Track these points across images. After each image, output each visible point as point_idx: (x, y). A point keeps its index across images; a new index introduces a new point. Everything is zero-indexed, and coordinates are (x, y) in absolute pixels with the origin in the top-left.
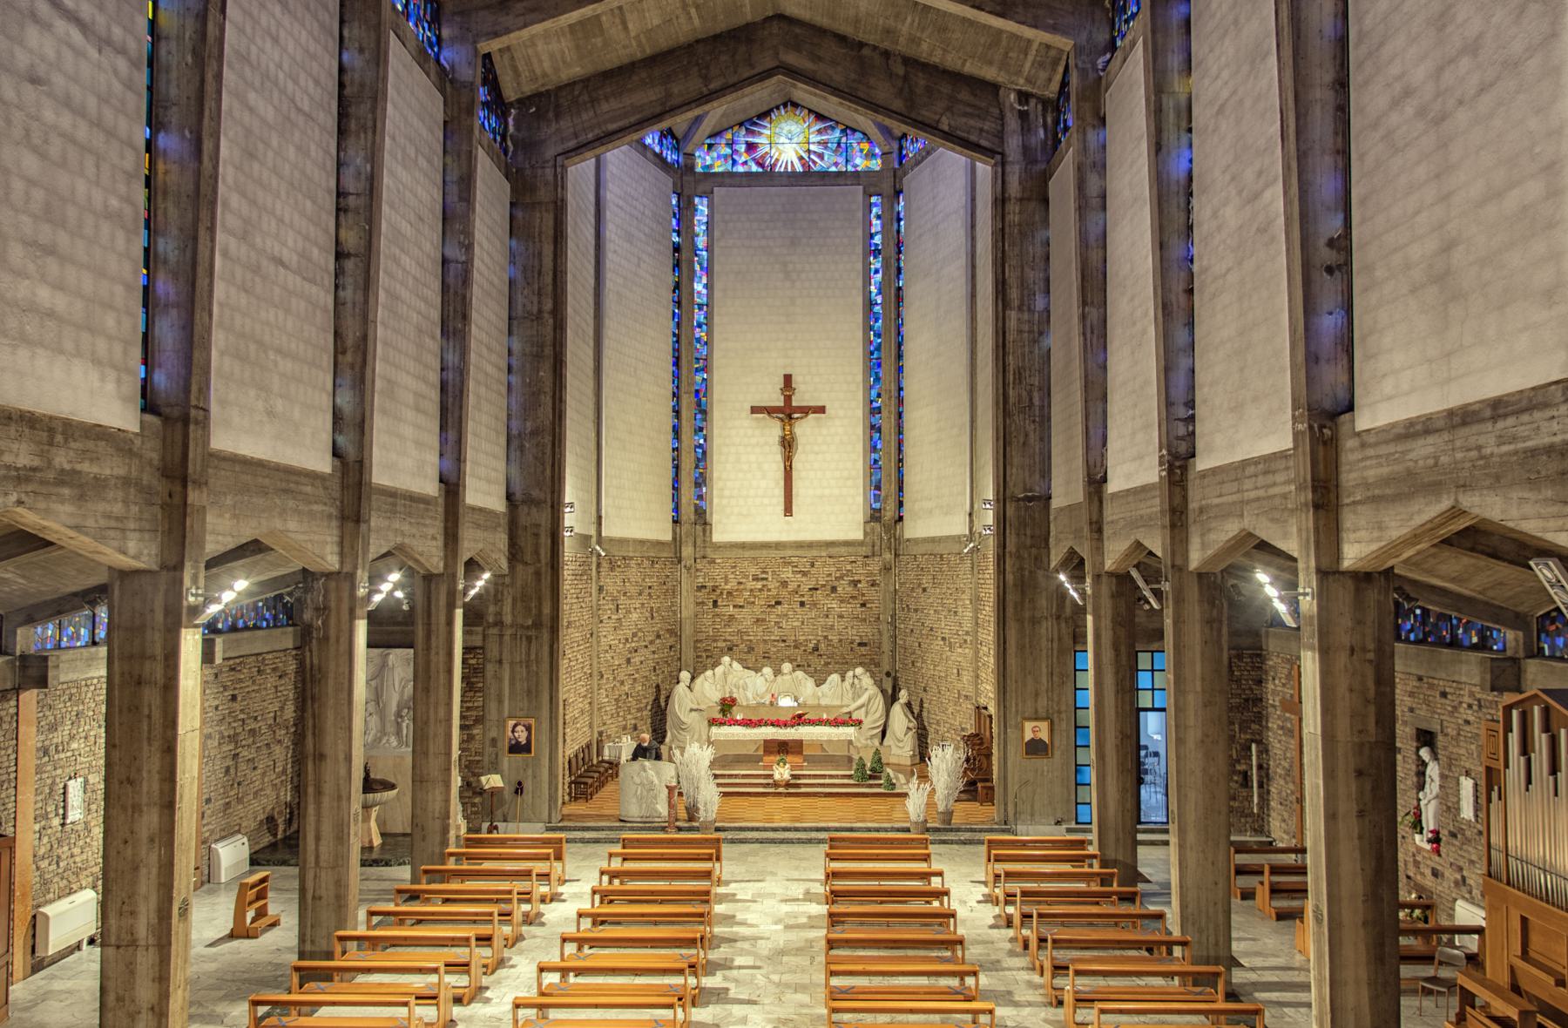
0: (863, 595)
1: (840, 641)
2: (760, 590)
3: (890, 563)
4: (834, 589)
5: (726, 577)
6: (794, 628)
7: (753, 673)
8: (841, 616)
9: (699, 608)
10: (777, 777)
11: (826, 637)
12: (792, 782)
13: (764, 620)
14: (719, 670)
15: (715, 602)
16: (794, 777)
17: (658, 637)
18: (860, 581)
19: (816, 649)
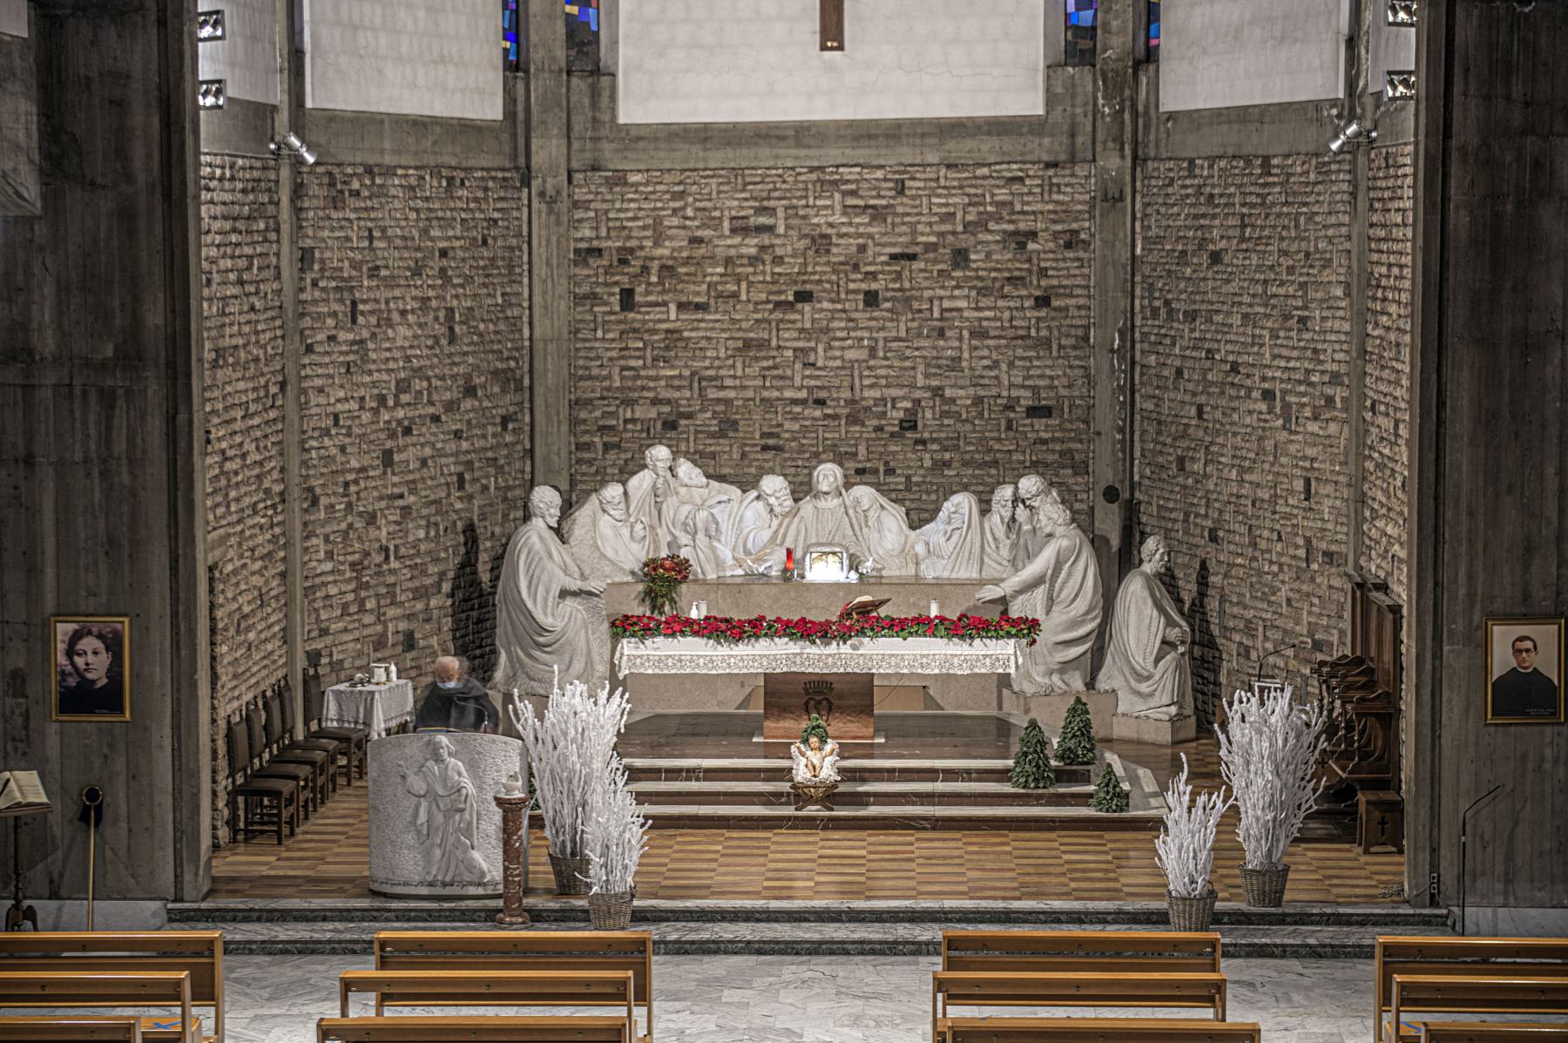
0: (1043, 273)
1: (978, 401)
2: (753, 260)
3: (1118, 181)
4: (960, 257)
5: (658, 221)
6: (849, 366)
7: (735, 492)
8: (980, 333)
9: (581, 312)
10: (802, 774)
11: (937, 392)
12: (842, 788)
13: (764, 344)
14: (641, 482)
16: (849, 774)
17: (470, 391)
18: (1033, 235)
19: (909, 424)
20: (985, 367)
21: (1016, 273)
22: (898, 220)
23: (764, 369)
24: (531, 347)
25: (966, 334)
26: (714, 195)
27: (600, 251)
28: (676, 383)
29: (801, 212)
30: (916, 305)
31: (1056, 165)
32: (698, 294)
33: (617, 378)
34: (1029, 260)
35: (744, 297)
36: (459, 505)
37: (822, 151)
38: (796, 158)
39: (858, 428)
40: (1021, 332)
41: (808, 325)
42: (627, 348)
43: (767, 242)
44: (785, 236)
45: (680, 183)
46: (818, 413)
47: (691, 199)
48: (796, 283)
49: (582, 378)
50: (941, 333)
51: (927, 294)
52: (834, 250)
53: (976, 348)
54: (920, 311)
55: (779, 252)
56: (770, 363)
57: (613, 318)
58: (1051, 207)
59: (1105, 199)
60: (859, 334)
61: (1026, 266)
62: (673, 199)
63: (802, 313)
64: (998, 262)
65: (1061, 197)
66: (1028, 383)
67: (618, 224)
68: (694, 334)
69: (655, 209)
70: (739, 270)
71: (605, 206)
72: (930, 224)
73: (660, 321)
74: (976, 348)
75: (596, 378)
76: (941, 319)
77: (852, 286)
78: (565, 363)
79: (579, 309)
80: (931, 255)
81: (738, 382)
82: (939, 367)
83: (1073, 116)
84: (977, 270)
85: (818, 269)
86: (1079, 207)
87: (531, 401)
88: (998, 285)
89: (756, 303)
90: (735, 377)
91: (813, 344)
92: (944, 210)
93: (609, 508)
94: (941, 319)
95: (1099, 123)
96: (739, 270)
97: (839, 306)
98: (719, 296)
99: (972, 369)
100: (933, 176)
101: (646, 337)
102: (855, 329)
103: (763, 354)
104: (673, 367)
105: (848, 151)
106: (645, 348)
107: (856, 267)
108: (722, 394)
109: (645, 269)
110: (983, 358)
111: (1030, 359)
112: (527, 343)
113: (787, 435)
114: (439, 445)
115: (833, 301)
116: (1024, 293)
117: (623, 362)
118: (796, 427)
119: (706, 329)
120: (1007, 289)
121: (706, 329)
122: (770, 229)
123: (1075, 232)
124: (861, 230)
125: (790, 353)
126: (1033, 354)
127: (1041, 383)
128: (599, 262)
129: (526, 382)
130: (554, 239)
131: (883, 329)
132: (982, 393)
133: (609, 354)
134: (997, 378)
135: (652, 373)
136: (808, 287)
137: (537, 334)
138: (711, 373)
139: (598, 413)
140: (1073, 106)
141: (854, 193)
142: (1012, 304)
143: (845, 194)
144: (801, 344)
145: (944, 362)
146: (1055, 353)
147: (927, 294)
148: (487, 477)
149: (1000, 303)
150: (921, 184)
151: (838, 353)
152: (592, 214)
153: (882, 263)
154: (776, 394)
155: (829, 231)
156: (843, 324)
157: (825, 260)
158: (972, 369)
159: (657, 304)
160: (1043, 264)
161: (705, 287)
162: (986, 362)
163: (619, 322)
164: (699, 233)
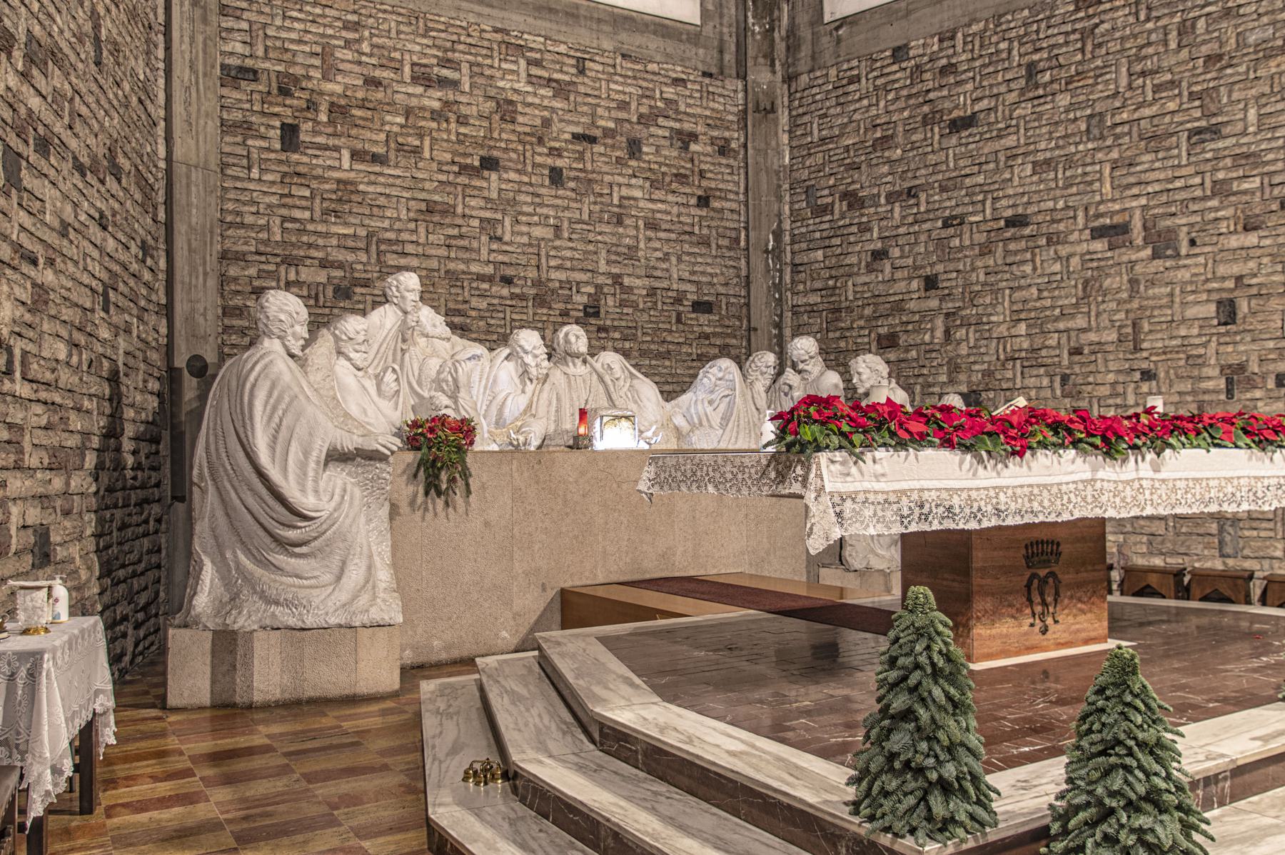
0: (702, 174)
1: (652, 292)
2: (436, 115)
4: (634, 147)
6: (536, 243)
8: (652, 225)
11: (617, 279)
13: (448, 211)
15: (290, 134)
18: (693, 137)
21: (682, 171)
22: (579, 99)
23: (450, 237)
24: (169, 172)
25: (641, 223)
26: (393, 34)
27: (255, 72)
28: (350, 243)
29: (488, 72)
30: (597, 189)
31: (711, 75)
32: (376, 142)
34: (692, 160)
35: (427, 154)
37: (506, 14)
38: (479, 15)
39: (545, 311)
40: (687, 228)
41: (494, 195)
42: (290, 195)
43: (451, 97)
44: (471, 94)
45: (355, 12)
46: (505, 292)
47: (366, 33)
48: (482, 146)
49: (231, 225)
50: (620, 223)
51: (607, 178)
52: (520, 119)
53: (650, 239)
54: (601, 195)
55: (464, 110)
56: (455, 232)
57: (273, 156)
58: (708, 113)
59: (757, 110)
60: (545, 211)
61: (689, 165)
62: (345, 28)
63: (487, 180)
64: (666, 158)
65: (716, 106)
66: (693, 278)
67: (278, 44)
68: (371, 189)
69: (323, 35)
70: (423, 123)
71: (262, 19)
72: (609, 109)
73: (330, 168)
74: (650, 239)
75: (251, 226)
76: (620, 206)
77: (538, 159)
78: (213, 200)
79: (228, 139)
80: (609, 141)
82: (618, 254)
83: (721, 33)
84: (649, 162)
85: (504, 136)
86: (730, 118)
88: (667, 179)
89: (440, 163)
90: (416, 243)
91: (499, 216)
92: (622, 97)
93: (348, 349)
94: (620, 206)
95: (749, 40)
96: (423, 123)
97: (526, 179)
98: (400, 147)
100: (610, 61)
101: (314, 184)
102: (541, 205)
104: (346, 224)
105: (530, 20)
106: (312, 197)
107: (540, 141)
109: (311, 106)
110: (656, 250)
112: (162, 165)
113: (473, 313)
114: (83, 217)
115: (518, 171)
116: (688, 190)
117: (284, 212)
118: (483, 304)
119: (385, 185)
120: (674, 186)
121: (385, 185)
122: (455, 84)
123: (727, 140)
124: (546, 103)
125: (476, 223)
126: (696, 250)
127: (704, 279)
128: (253, 86)
130: (200, 38)
131: (568, 208)
132: (657, 284)
133: (267, 199)
134: (667, 270)
135: (321, 228)
136: (495, 153)
137: (178, 153)
139: (252, 271)
140: (721, 24)
141: (537, 63)
142: (679, 199)
143: (530, 62)
144: (488, 214)
146: (714, 252)
147: (607, 178)
149: (670, 198)
150: (600, 68)
151: (525, 229)
152: (245, 26)
153: (566, 141)
154: (462, 267)
155: (515, 98)
156: (529, 199)
157: (510, 127)
159: (326, 148)
160: (703, 167)
161: (382, 137)
162: (658, 254)
163: (280, 162)
164: (378, 73)
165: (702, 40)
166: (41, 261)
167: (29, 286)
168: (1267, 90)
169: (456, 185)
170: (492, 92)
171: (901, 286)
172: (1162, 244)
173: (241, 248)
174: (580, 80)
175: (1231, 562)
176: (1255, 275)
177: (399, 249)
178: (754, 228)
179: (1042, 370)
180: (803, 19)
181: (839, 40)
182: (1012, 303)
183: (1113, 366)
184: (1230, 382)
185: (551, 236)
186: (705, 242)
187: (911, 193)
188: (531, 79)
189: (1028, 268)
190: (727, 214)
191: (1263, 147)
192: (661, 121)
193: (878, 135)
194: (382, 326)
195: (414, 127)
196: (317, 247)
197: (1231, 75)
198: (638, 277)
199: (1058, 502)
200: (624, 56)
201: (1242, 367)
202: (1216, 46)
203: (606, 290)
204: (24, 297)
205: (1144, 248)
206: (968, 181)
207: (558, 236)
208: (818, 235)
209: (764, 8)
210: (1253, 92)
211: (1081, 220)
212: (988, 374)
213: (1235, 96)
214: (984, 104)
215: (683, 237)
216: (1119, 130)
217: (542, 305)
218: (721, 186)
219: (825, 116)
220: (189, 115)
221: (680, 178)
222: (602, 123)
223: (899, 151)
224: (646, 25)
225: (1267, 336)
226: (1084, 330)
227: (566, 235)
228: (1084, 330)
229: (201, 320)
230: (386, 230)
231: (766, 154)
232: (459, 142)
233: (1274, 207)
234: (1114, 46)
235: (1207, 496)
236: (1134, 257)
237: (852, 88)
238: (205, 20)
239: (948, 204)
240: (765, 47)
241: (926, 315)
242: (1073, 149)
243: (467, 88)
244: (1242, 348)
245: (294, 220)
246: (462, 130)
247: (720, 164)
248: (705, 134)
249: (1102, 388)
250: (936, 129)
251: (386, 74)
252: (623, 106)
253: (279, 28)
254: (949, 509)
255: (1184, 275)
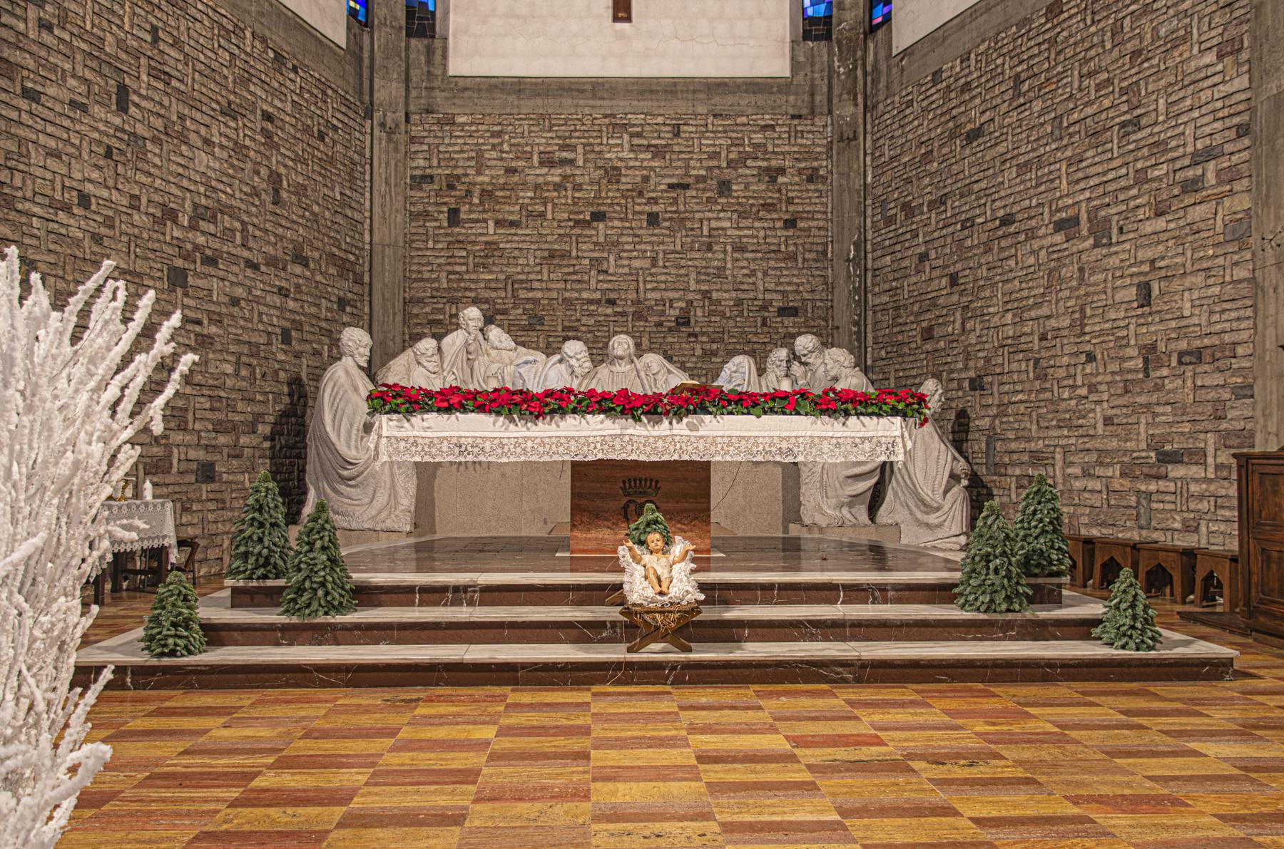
0: (790, 201)
1: (739, 302)
2: (558, 187)
3: (851, 125)
5: (480, 154)
6: (634, 273)
7: (540, 357)
9: (415, 227)
10: (639, 590)
11: (706, 295)
12: (708, 614)
13: (566, 255)
14: (454, 341)
15: (454, 216)
16: (715, 593)
18: (782, 171)
19: (683, 321)
20: (744, 275)
21: (769, 201)
22: (674, 157)
25: (729, 248)
26: (526, 134)
27: (431, 177)
28: (494, 285)
29: (597, 149)
30: (689, 224)
31: (800, 117)
32: (512, 213)
33: (444, 281)
34: (780, 191)
35: (549, 216)
36: (282, 357)
37: (614, 103)
38: (593, 107)
40: (773, 248)
41: (601, 240)
42: (453, 256)
43: (569, 172)
44: (584, 167)
45: (499, 124)
46: (609, 311)
47: (507, 137)
48: (592, 205)
49: (415, 280)
50: (709, 248)
51: (698, 216)
52: (623, 180)
53: (737, 260)
54: (692, 229)
55: (578, 180)
56: (571, 270)
57: (442, 231)
58: (796, 149)
59: (841, 140)
60: (643, 247)
61: (777, 195)
62: (492, 136)
63: (596, 229)
64: (754, 192)
65: (804, 141)
67: (447, 156)
68: (508, 246)
69: (477, 144)
70: (547, 194)
71: (436, 141)
72: (701, 160)
73: (481, 234)
74: (737, 260)
75: (427, 280)
76: (710, 236)
77: (638, 208)
78: (400, 266)
79: (414, 224)
80: (701, 186)
81: (544, 285)
82: (708, 275)
83: (813, 79)
84: (738, 198)
85: (610, 194)
86: (819, 149)
87: (370, 295)
88: (754, 209)
89: (560, 221)
91: (605, 255)
92: (712, 149)
94: (710, 236)
95: (835, 81)
96: (547, 194)
97: (627, 225)
98: (530, 215)
99: (734, 276)
100: (702, 122)
101: (469, 247)
102: (640, 243)
103: (565, 262)
104: (491, 272)
105: (635, 103)
106: (468, 256)
107: (641, 194)
108: (531, 295)
109: (469, 193)
110: (743, 268)
111: (780, 269)
112: (367, 247)
113: (584, 329)
115: (621, 220)
116: (775, 216)
117: (449, 268)
118: (592, 322)
119: (518, 242)
120: (761, 214)
121: (518, 242)
122: (572, 162)
123: (815, 169)
124: (645, 164)
125: (587, 262)
126: (783, 265)
127: (790, 288)
128: (431, 186)
129: (367, 279)
130: (392, 163)
131: (663, 243)
132: (742, 296)
134: (754, 284)
135: (473, 276)
136: (602, 208)
137: (376, 238)
138: (523, 277)
140: (813, 72)
141: (639, 135)
142: (766, 225)
143: (632, 135)
144: (596, 255)
145: (712, 271)
146: (800, 265)
147: (698, 216)
148: (322, 344)
149: (757, 224)
150: (694, 129)
151: (626, 262)
152: (425, 148)
153: (662, 191)
154: (575, 295)
155: (619, 164)
156: (630, 239)
157: (616, 187)
158: (734, 276)
159: (477, 221)
160: (790, 194)
161: (517, 208)
162: (746, 271)
163: (447, 235)
164: (514, 164)
165: (793, 88)
166: (206, 322)
167: (192, 336)
168: (1172, 80)
169: (570, 236)
170: (601, 163)
171: (935, 284)
172: (1101, 232)
173: (421, 294)
174: (675, 141)
175: (1144, 533)
176: (1163, 258)
177: (528, 286)
178: (838, 241)
179: (1021, 356)
180: (882, 54)
181: (903, 70)
182: (1004, 294)
183: (1067, 350)
184: (1146, 361)
185: (648, 265)
186: (792, 257)
187: (942, 201)
188: (633, 148)
189: (1012, 263)
190: (814, 232)
191: (1169, 134)
192: (749, 162)
193: (923, 151)
194: (454, 343)
195: (541, 197)
196: (470, 290)
197: (1148, 68)
198: (725, 291)
199: (585, 449)
200: (715, 116)
201: (1153, 347)
202: (1137, 42)
203: (695, 304)
204: (187, 342)
205: (1088, 237)
206: (976, 187)
207: (654, 265)
208: (887, 243)
209: (848, 51)
210: (1163, 82)
211: (1046, 217)
212: (987, 359)
213: (1150, 89)
214: (987, 116)
215: (768, 255)
216: (1071, 130)
217: (639, 319)
218: (807, 209)
219: (892, 137)
220: (384, 212)
221: (767, 206)
222: (693, 172)
223: (935, 164)
224: (739, 86)
225: (1170, 316)
226: (1048, 317)
227: (661, 263)
228: (1048, 317)
229: (391, 344)
230: (519, 273)
231: (849, 176)
232: (575, 204)
233: (1176, 192)
234: (1069, 52)
235: (755, 449)
236: (1081, 248)
237: (908, 111)
238: (396, 150)
239: (964, 208)
240: (849, 85)
241: (951, 309)
242: (1042, 151)
243: (581, 163)
244: (1152, 329)
245: (457, 273)
246: (577, 195)
247: (807, 191)
248: (793, 167)
249: (1060, 370)
250: (958, 142)
251: (520, 163)
252: (715, 155)
253: (448, 145)
254: (483, 449)
255: (1114, 261)
